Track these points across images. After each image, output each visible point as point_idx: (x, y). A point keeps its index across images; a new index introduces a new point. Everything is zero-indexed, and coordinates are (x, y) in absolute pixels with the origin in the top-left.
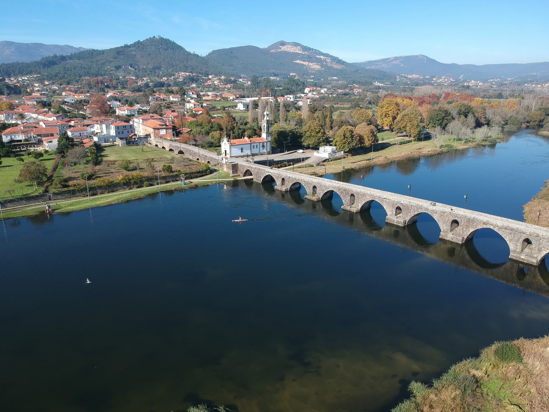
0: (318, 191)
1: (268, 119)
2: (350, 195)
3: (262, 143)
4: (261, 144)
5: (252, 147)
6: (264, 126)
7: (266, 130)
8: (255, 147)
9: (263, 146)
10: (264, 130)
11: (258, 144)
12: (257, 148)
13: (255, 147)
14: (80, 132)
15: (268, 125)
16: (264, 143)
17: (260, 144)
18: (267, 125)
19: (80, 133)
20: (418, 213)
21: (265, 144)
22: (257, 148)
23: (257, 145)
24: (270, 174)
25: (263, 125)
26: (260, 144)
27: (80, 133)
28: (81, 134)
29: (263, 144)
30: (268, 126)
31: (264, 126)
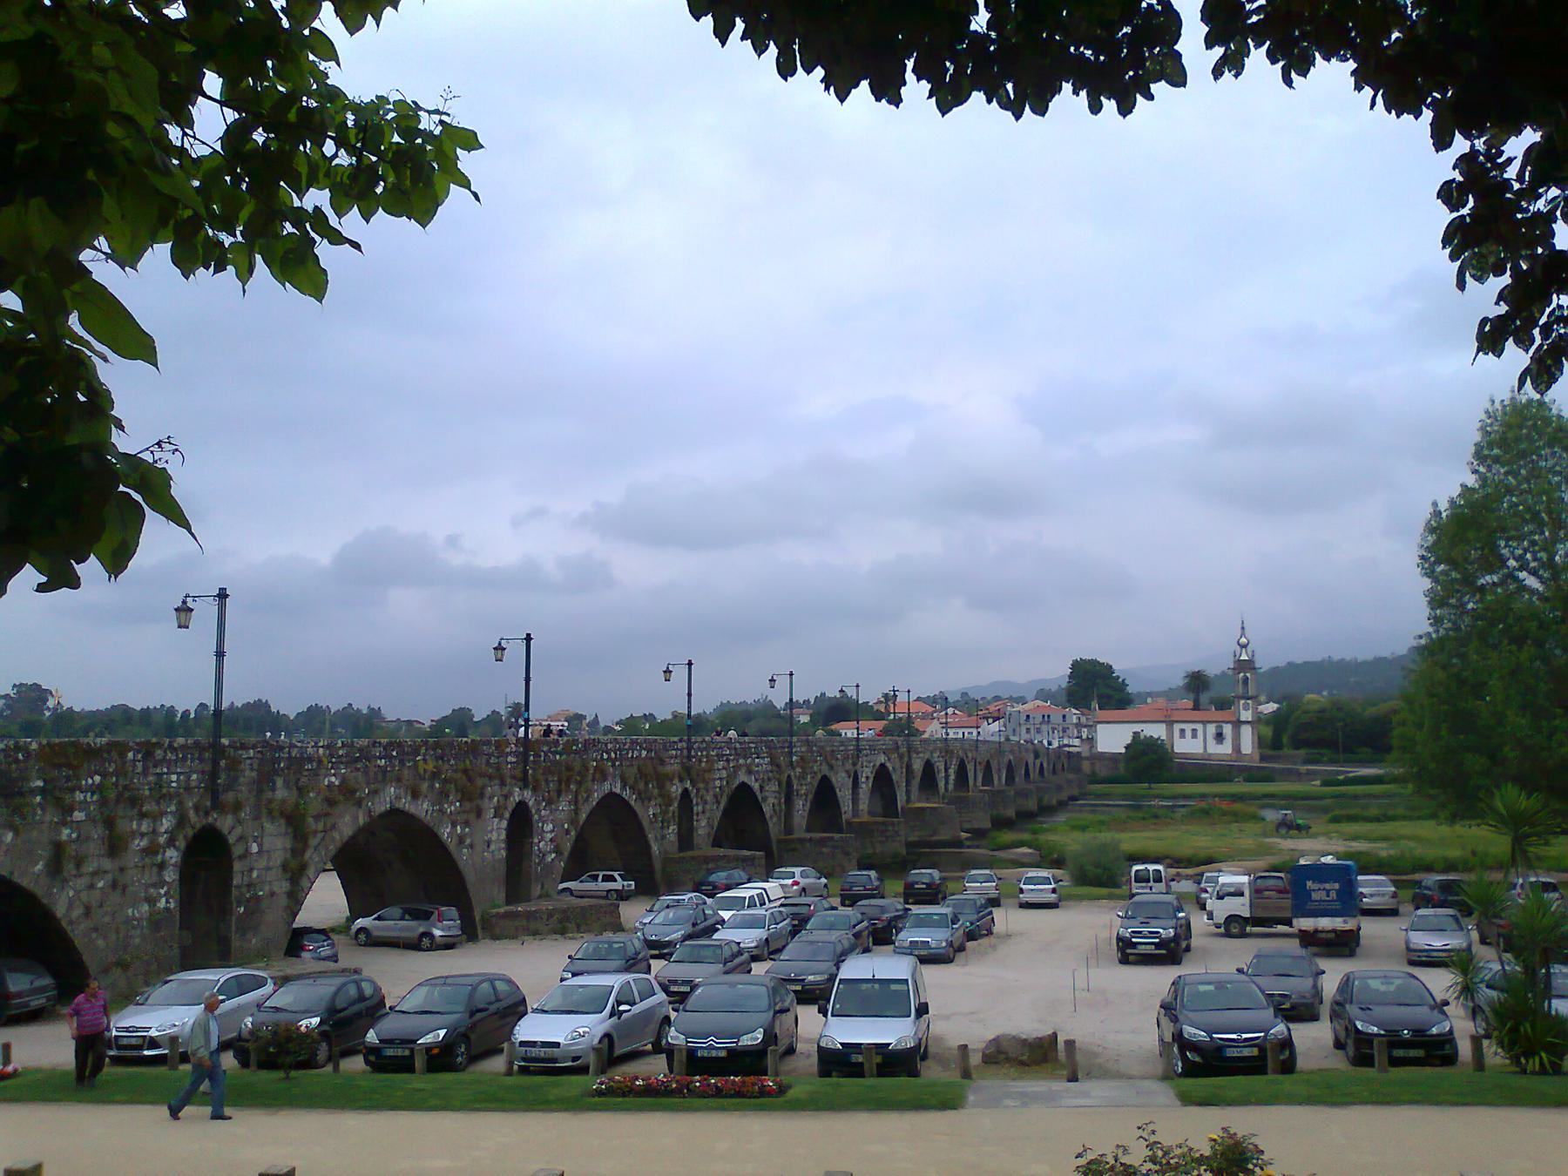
3: (1215, 725)
4: (1211, 729)
5: (1177, 734)
8: (1188, 734)
9: (1219, 737)
11: (1199, 727)
12: (1194, 735)
13: (1188, 734)
14: (963, 730)
16: (1222, 727)
19: (963, 733)
21: (1228, 730)
22: (1194, 735)
23: (1194, 731)
27: (963, 733)
28: (966, 734)
29: (1217, 727)
30: (1246, 680)
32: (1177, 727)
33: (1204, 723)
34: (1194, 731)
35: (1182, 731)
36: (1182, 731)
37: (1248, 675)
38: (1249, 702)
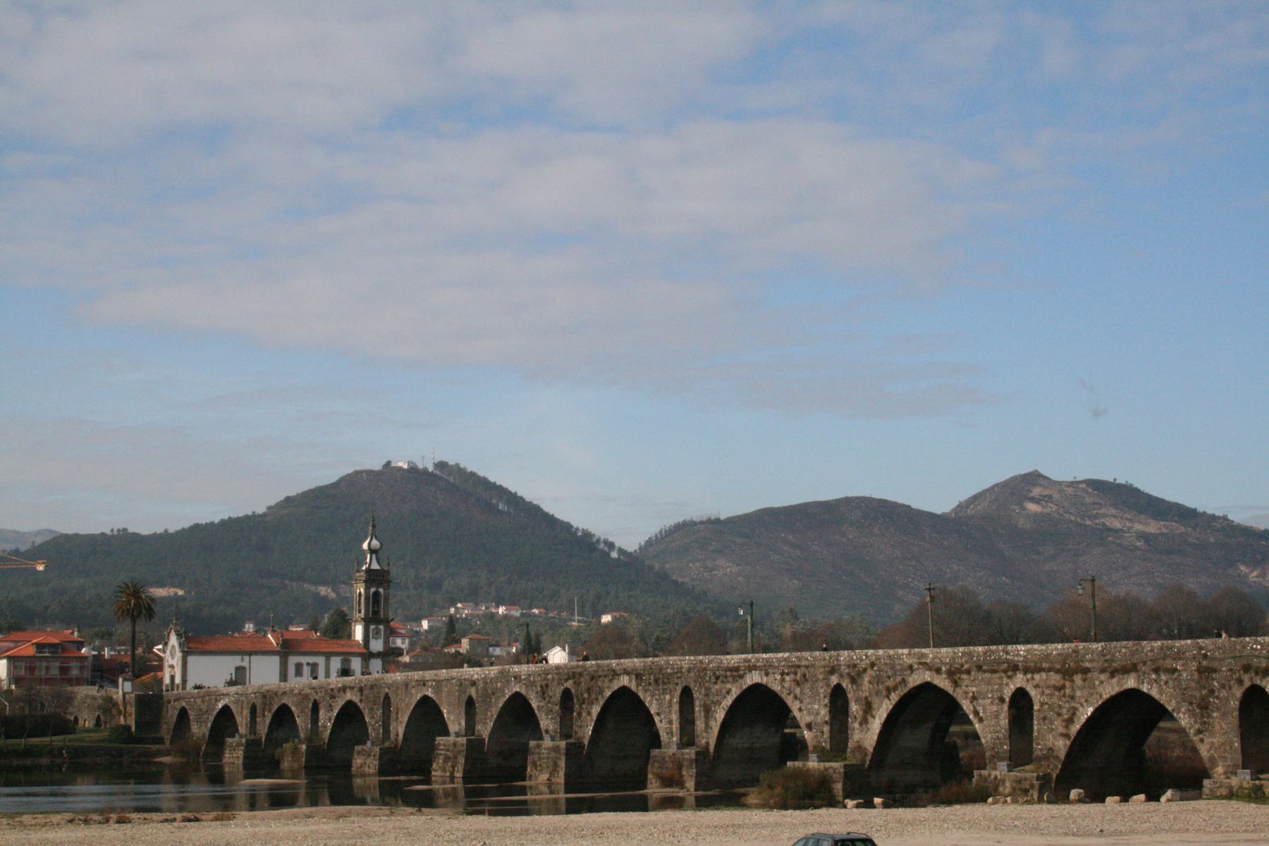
1: (375, 566)
4: (336, 663)
6: (360, 593)
7: (363, 611)
8: (306, 670)
10: (360, 612)
11: (320, 660)
13: (306, 670)
15: (373, 590)
17: (328, 660)
18: (367, 589)
20: (505, 700)
25: (358, 590)
26: (328, 660)
30: (376, 594)
31: (360, 593)
32: (293, 660)
33: (328, 655)
34: (314, 667)
37: (381, 590)
38: (381, 627)
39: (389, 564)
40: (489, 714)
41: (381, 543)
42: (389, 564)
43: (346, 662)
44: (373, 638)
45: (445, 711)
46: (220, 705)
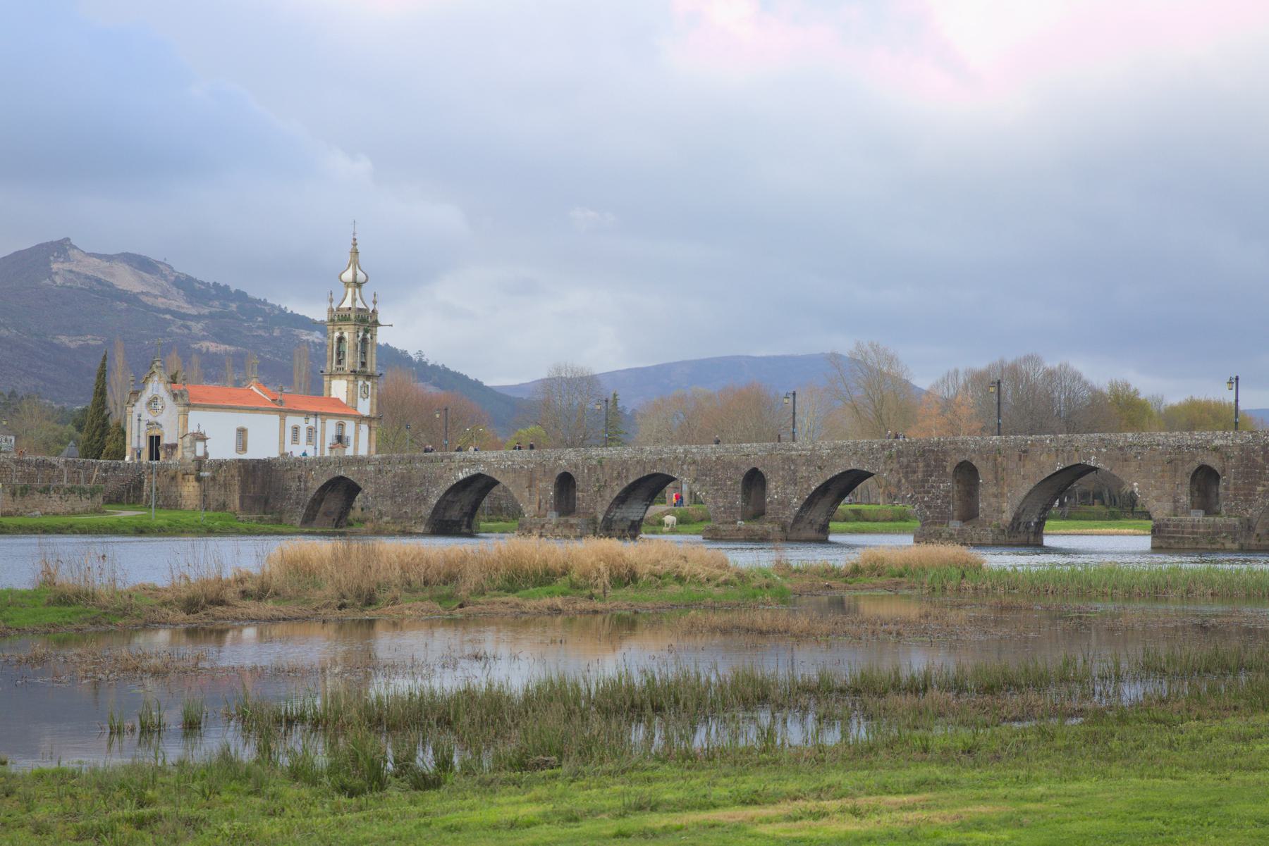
0: (774, 491)
2: (949, 469)
3: (336, 421)
6: (341, 339)
8: (303, 435)
13: (303, 435)
17: (323, 422)
24: (481, 469)
25: (337, 334)
31: (341, 339)
32: (292, 421)
35: (296, 430)
36: (296, 430)
38: (368, 383)
39: (375, 302)
40: (1260, 489)
41: (367, 276)
42: (375, 302)
43: (341, 426)
44: (361, 397)
45: (1135, 484)
46: (461, 476)
